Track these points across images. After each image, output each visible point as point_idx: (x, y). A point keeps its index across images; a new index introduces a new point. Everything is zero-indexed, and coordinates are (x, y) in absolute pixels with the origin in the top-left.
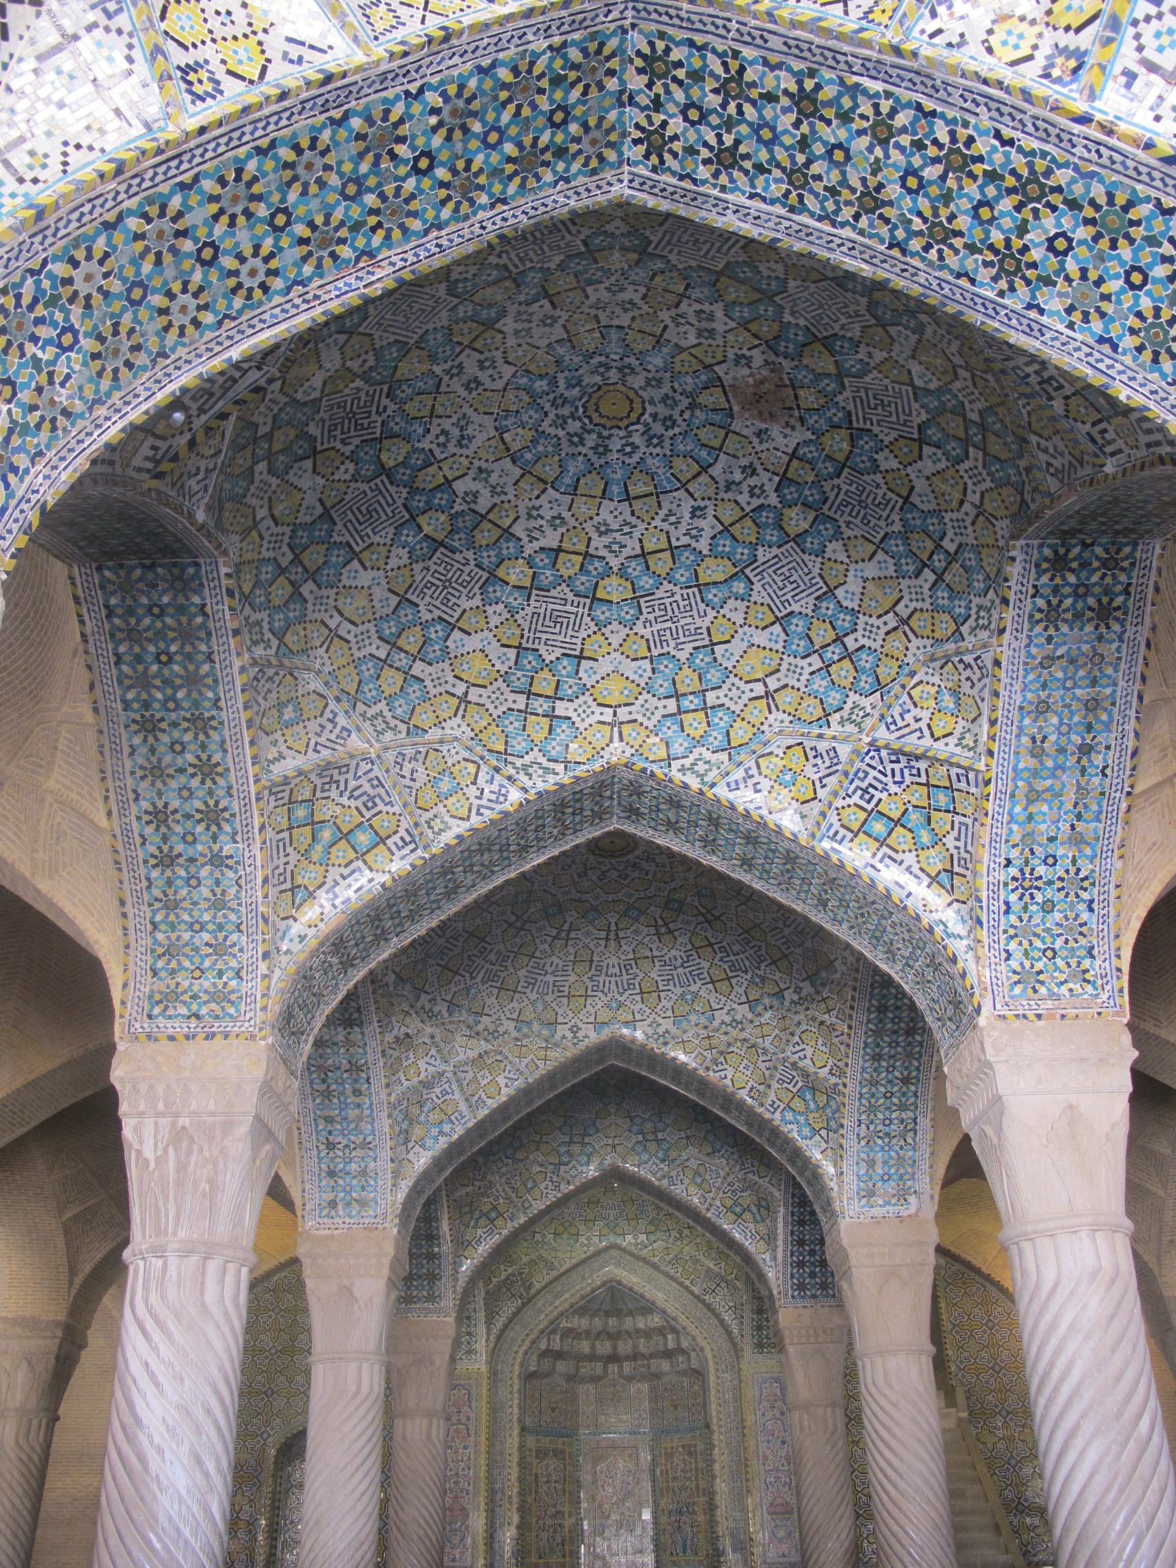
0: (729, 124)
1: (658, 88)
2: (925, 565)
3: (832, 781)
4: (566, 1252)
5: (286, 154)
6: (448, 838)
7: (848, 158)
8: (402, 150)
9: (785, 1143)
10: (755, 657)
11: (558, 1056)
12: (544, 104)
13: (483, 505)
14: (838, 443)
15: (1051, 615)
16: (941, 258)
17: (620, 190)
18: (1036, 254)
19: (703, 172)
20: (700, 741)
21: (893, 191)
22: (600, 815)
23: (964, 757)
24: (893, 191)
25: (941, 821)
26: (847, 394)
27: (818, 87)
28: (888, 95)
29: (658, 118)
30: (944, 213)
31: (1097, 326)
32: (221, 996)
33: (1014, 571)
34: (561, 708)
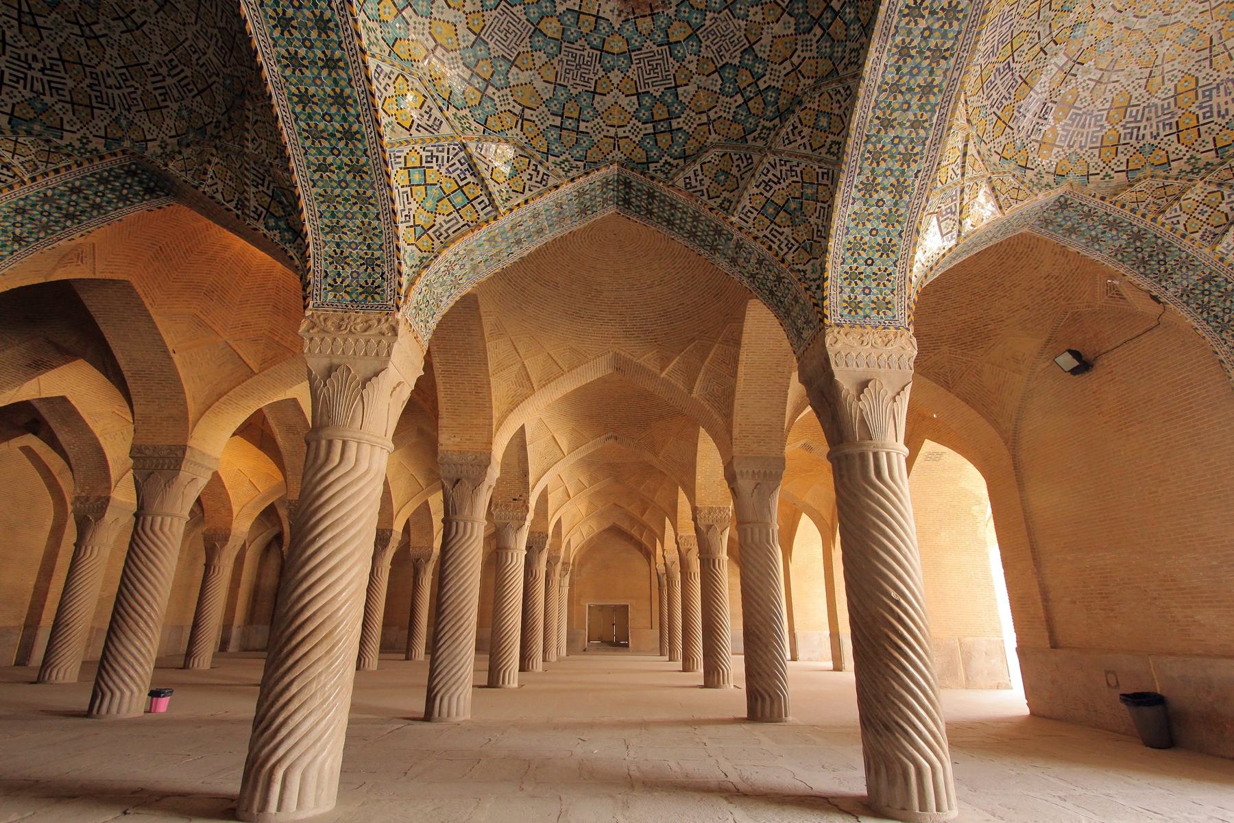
0: (920, 52)
1: (941, 14)
2: (562, 116)
3: (424, 134)
7: (904, 111)
14: (617, 45)
16: (867, 159)
18: (876, 196)
19: (898, 39)
21: (892, 133)
24: (892, 133)
25: (445, 206)
26: (655, 48)
27: (934, 94)
28: (931, 125)
29: (926, 13)
30: (886, 156)
31: (852, 225)
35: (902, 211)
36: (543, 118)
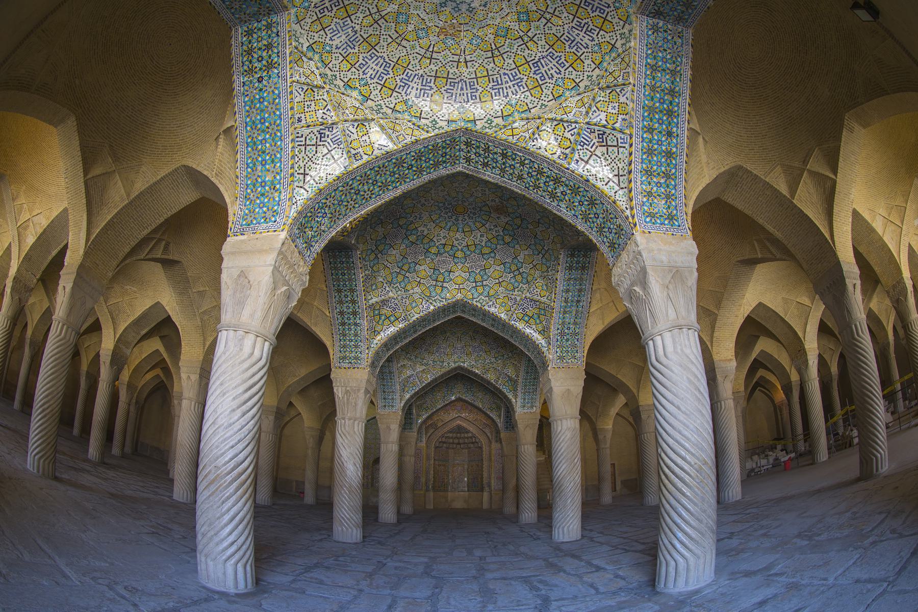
0: (486, 158)
4: (447, 417)
5: (377, 169)
6: (414, 318)
8: (405, 165)
9: (503, 394)
10: (496, 273)
11: (444, 370)
12: (440, 152)
13: (425, 233)
14: (518, 221)
15: (570, 268)
17: (460, 169)
19: (480, 167)
20: (481, 294)
22: (455, 312)
23: (548, 302)
24: (525, 176)
32: (356, 358)
33: (561, 257)
34: (445, 285)
35: (571, 183)
36: (538, 259)
